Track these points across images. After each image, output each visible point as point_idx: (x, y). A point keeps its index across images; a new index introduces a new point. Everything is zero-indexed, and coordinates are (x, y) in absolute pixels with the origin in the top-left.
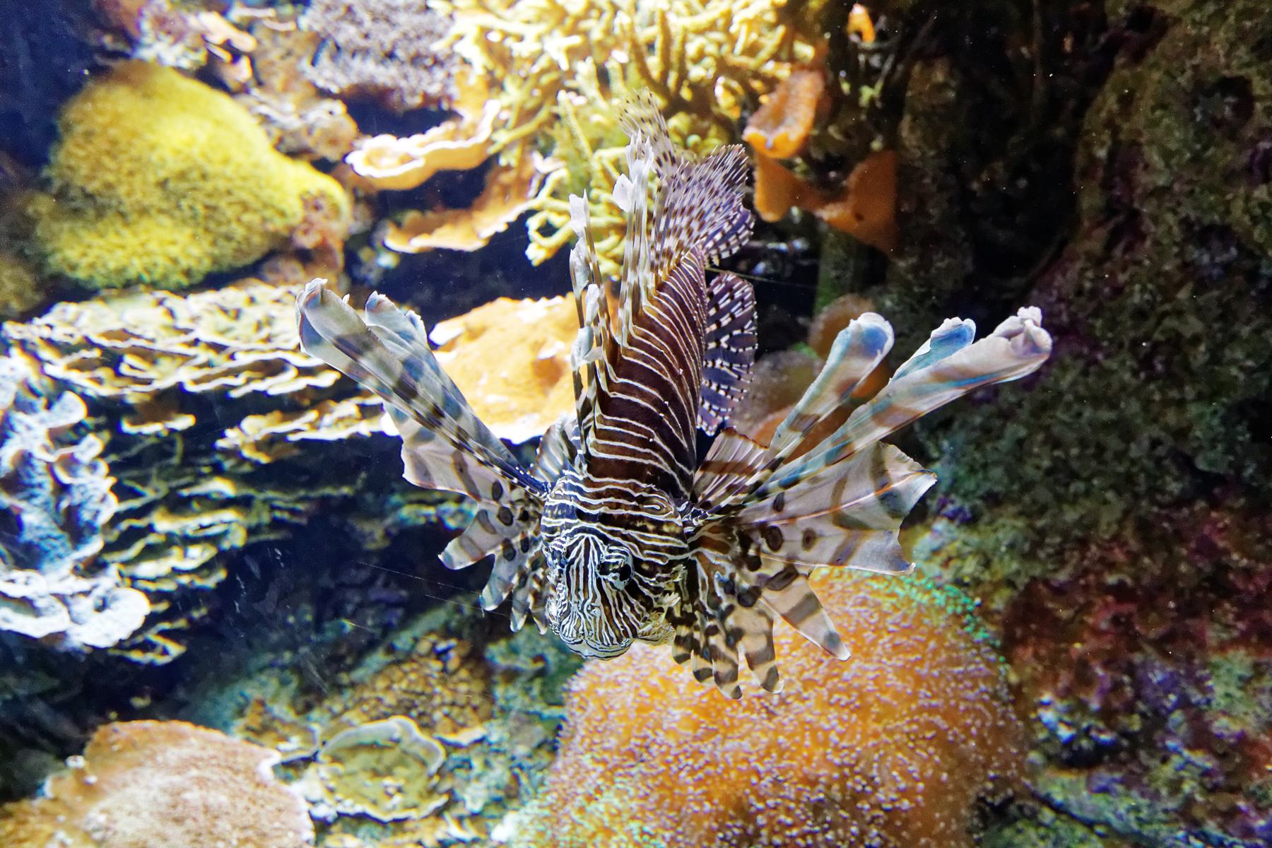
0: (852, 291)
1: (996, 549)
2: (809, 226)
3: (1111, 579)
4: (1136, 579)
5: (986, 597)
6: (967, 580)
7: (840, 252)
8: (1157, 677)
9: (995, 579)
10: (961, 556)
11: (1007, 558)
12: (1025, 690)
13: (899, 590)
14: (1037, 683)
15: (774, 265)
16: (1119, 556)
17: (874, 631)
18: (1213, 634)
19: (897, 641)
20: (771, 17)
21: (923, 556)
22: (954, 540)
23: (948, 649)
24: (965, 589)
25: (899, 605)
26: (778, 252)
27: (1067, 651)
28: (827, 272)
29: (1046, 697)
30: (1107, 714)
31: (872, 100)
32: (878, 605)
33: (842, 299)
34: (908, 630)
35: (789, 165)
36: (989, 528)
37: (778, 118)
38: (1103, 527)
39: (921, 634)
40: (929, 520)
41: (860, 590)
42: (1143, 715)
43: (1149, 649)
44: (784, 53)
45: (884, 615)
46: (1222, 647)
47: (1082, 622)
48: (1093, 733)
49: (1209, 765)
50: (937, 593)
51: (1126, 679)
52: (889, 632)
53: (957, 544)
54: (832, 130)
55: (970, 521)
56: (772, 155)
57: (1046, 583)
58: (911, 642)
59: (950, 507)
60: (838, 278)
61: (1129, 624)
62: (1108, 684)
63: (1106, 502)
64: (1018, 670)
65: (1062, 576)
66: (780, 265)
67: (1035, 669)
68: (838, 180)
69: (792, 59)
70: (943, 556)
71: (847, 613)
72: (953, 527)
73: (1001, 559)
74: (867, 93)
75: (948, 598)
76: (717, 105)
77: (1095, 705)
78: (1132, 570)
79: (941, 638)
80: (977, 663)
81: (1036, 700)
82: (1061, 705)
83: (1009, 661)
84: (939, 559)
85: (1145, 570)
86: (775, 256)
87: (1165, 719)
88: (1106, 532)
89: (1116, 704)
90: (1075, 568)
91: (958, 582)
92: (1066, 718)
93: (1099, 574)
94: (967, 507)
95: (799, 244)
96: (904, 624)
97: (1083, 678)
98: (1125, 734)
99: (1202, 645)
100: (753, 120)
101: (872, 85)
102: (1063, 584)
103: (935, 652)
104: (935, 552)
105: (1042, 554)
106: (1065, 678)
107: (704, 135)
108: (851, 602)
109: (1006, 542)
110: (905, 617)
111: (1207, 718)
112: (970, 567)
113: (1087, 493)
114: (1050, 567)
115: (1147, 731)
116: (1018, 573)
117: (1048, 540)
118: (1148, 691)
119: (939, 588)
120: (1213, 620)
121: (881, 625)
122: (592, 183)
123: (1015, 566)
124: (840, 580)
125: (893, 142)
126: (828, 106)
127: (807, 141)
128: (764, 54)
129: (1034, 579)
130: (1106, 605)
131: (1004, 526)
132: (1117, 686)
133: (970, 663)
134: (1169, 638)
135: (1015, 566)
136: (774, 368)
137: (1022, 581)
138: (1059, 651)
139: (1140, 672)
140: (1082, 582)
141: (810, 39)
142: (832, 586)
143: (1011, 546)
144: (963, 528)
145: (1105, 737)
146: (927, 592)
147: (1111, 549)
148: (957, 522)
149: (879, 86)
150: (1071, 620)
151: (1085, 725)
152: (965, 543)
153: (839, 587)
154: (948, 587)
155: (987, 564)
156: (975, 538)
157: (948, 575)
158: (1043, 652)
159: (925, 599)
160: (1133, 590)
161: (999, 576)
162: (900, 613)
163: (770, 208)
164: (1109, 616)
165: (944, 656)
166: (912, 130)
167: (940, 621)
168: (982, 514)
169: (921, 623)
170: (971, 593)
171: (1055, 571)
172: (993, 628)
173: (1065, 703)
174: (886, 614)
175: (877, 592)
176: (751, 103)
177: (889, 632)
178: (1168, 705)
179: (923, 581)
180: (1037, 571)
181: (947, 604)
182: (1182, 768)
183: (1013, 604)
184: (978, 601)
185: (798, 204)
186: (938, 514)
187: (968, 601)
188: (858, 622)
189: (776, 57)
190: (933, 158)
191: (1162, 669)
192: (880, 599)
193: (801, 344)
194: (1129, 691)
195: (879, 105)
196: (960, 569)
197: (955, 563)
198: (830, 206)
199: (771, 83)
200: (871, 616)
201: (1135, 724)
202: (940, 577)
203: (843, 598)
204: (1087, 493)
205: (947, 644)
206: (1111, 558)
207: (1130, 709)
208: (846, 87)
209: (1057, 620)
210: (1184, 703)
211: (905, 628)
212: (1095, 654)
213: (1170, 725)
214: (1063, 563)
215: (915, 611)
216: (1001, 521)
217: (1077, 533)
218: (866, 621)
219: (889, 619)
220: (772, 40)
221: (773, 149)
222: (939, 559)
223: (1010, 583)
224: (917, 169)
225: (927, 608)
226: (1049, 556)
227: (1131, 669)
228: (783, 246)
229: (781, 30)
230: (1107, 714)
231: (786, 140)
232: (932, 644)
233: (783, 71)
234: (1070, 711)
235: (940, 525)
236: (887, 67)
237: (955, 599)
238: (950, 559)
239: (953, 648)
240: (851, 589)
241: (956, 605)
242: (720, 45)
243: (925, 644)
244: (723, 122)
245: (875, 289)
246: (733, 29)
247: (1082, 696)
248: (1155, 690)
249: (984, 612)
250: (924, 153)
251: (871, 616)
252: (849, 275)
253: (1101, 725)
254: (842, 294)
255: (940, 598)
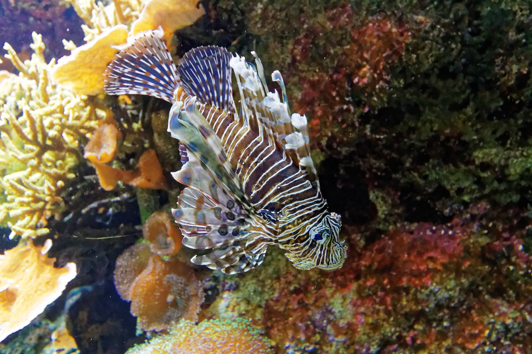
0: (156, 210)
1: (250, 294)
2: (129, 189)
3: (292, 288)
4: (299, 284)
5: (253, 316)
6: (243, 312)
7: (146, 195)
8: (318, 317)
9: (253, 307)
10: (238, 304)
11: (254, 296)
12: (280, 346)
13: (218, 329)
14: (282, 341)
15: (117, 208)
16: (291, 278)
17: (212, 351)
18: (328, 292)
19: (223, 350)
20: (82, 104)
21: (223, 311)
22: (233, 298)
23: (244, 344)
24: (244, 316)
25: (219, 335)
26: (117, 202)
27: (287, 323)
28: (142, 205)
29: (287, 344)
30: (308, 339)
31: (139, 129)
32: (211, 340)
33: (153, 215)
34: (225, 344)
35: (110, 163)
36: (244, 288)
37: (99, 145)
38: (282, 270)
39: (232, 342)
40: (221, 295)
41: (201, 337)
42: (319, 333)
43: (312, 308)
44: (92, 116)
45: (214, 342)
46: (332, 296)
47: (289, 309)
48: (307, 349)
49: (343, 339)
50: (233, 323)
51: (309, 323)
52: (219, 348)
53: (235, 300)
54: (125, 143)
55: (236, 288)
56: (100, 162)
57: (272, 300)
58: (229, 348)
59: (227, 286)
60: (148, 206)
61: (303, 302)
62: (304, 328)
63: (279, 260)
64: (274, 340)
65: (276, 295)
66: (120, 207)
67: (280, 336)
68: (134, 164)
69: (97, 118)
70: (231, 307)
71: (199, 350)
72: (231, 294)
73: (253, 298)
74: (136, 126)
75: (239, 323)
76: (67, 143)
77: (303, 338)
78: (296, 281)
79: (240, 340)
80: (256, 343)
81: (284, 348)
82: (293, 344)
83: (270, 337)
84: (230, 309)
85: (300, 280)
86: (116, 204)
87: (326, 330)
88: (284, 271)
89: (310, 334)
90: (279, 289)
91: (241, 315)
92: (296, 349)
93: (287, 288)
94: (233, 283)
95: (125, 195)
96: (224, 342)
97: (297, 330)
98: (317, 343)
99: (327, 298)
100: (87, 148)
101: (137, 122)
102: (277, 298)
103: (239, 347)
104: (228, 307)
105: (266, 290)
106: (290, 333)
107: (63, 159)
108: (199, 344)
109: (252, 291)
110: (223, 339)
111: (337, 323)
112: (243, 307)
113: (273, 259)
114: (271, 293)
115: (322, 338)
116: (260, 301)
117: (266, 283)
118: (317, 324)
119: (234, 321)
120: (326, 287)
121: (215, 347)
122: (6, 193)
123: (258, 298)
124: (192, 337)
125: (153, 145)
126: (120, 135)
127: (115, 153)
128: (83, 119)
129: (267, 300)
130: (294, 299)
131: (249, 284)
132: (307, 327)
133: (254, 345)
134: (316, 301)
135: (258, 298)
136: (131, 254)
137: (263, 303)
138: (285, 324)
139: (313, 318)
140: (283, 294)
141: (102, 108)
142: (189, 341)
143: (255, 292)
144: (235, 292)
145: (311, 348)
146: (230, 324)
147: (287, 277)
148: (232, 291)
149: (140, 122)
150: (285, 310)
151: (303, 347)
152: (238, 298)
153: (192, 340)
154: (237, 319)
155: (248, 302)
156: (240, 294)
157: (236, 314)
158: (280, 327)
159: (229, 328)
160: (299, 289)
161: (255, 305)
162: (221, 339)
163: (108, 184)
164: (296, 302)
165: (243, 347)
166: (160, 139)
167: (237, 334)
168: (240, 283)
169: (230, 338)
170: (247, 318)
171: (273, 294)
172: (259, 328)
173: (294, 343)
174: (215, 341)
175: (209, 334)
176: (83, 140)
177: (219, 348)
178: (325, 325)
179: (226, 321)
180: (267, 297)
181: (238, 325)
182: (337, 346)
183: (264, 314)
184: (250, 319)
185: (120, 179)
186: (223, 291)
187: (247, 320)
188: (205, 351)
189: (89, 119)
190: (171, 148)
191: (318, 313)
192: (211, 337)
193: (141, 239)
194: (312, 327)
195: (142, 130)
196: (240, 308)
197: (237, 308)
198: (135, 180)
199: (91, 130)
200: (210, 345)
201: (318, 338)
202: (233, 316)
203: (195, 343)
204: (273, 259)
205: (243, 342)
206: (289, 280)
207: (314, 333)
208: (125, 125)
209: (280, 312)
210: (329, 322)
211: (225, 343)
212: (296, 319)
213: (328, 332)
214: (274, 290)
215: (227, 335)
216: (247, 283)
217: (275, 276)
218: (208, 348)
219: (217, 343)
220: (85, 114)
221: (101, 159)
222: (230, 309)
223: (259, 306)
224: (167, 154)
225: (230, 331)
226: (269, 289)
227: (309, 318)
228: (118, 199)
229: (88, 108)
230: (308, 339)
231: (106, 154)
232: (237, 344)
233: (93, 123)
234: (297, 345)
235: (226, 295)
236: (141, 115)
237: (241, 322)
238: (234, 307)
239: (247, 342)
240: (198, 338)
241: (242, 325)
242: (61, 119)
243: (234, 345)
244: (72, 151)
245: (166, 206)
246: (65, 113)
247: (298, 337)
248: (319, 322)
249: (255, 322)
250: (167, 147)
251: (210, 345)
252: (153, 203)
253: (308, 344)
254: (153, 212)
255: (235, 325)
